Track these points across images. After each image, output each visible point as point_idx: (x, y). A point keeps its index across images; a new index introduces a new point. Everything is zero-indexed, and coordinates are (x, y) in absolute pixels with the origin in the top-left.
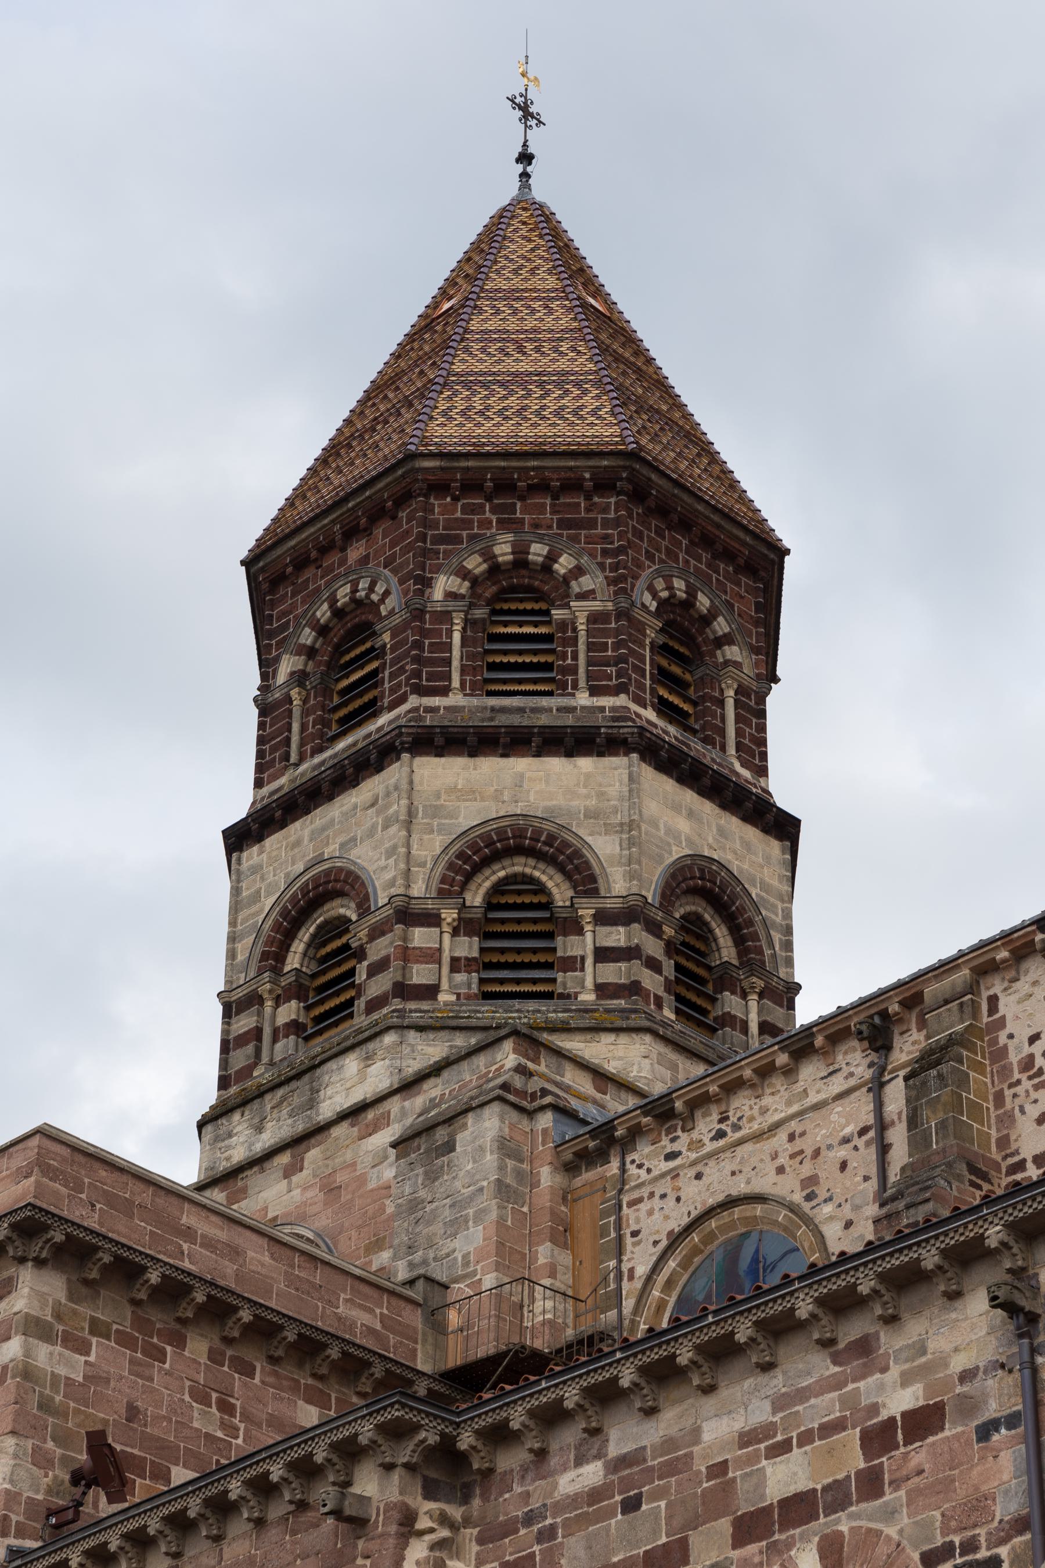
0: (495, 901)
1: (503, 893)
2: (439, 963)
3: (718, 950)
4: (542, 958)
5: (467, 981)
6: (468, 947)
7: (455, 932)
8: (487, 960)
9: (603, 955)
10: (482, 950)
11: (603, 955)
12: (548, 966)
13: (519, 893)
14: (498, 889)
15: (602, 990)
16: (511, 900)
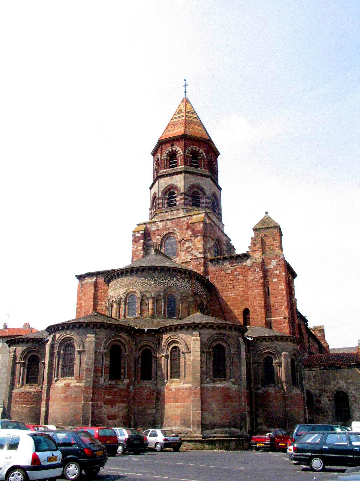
11: (181, 199)
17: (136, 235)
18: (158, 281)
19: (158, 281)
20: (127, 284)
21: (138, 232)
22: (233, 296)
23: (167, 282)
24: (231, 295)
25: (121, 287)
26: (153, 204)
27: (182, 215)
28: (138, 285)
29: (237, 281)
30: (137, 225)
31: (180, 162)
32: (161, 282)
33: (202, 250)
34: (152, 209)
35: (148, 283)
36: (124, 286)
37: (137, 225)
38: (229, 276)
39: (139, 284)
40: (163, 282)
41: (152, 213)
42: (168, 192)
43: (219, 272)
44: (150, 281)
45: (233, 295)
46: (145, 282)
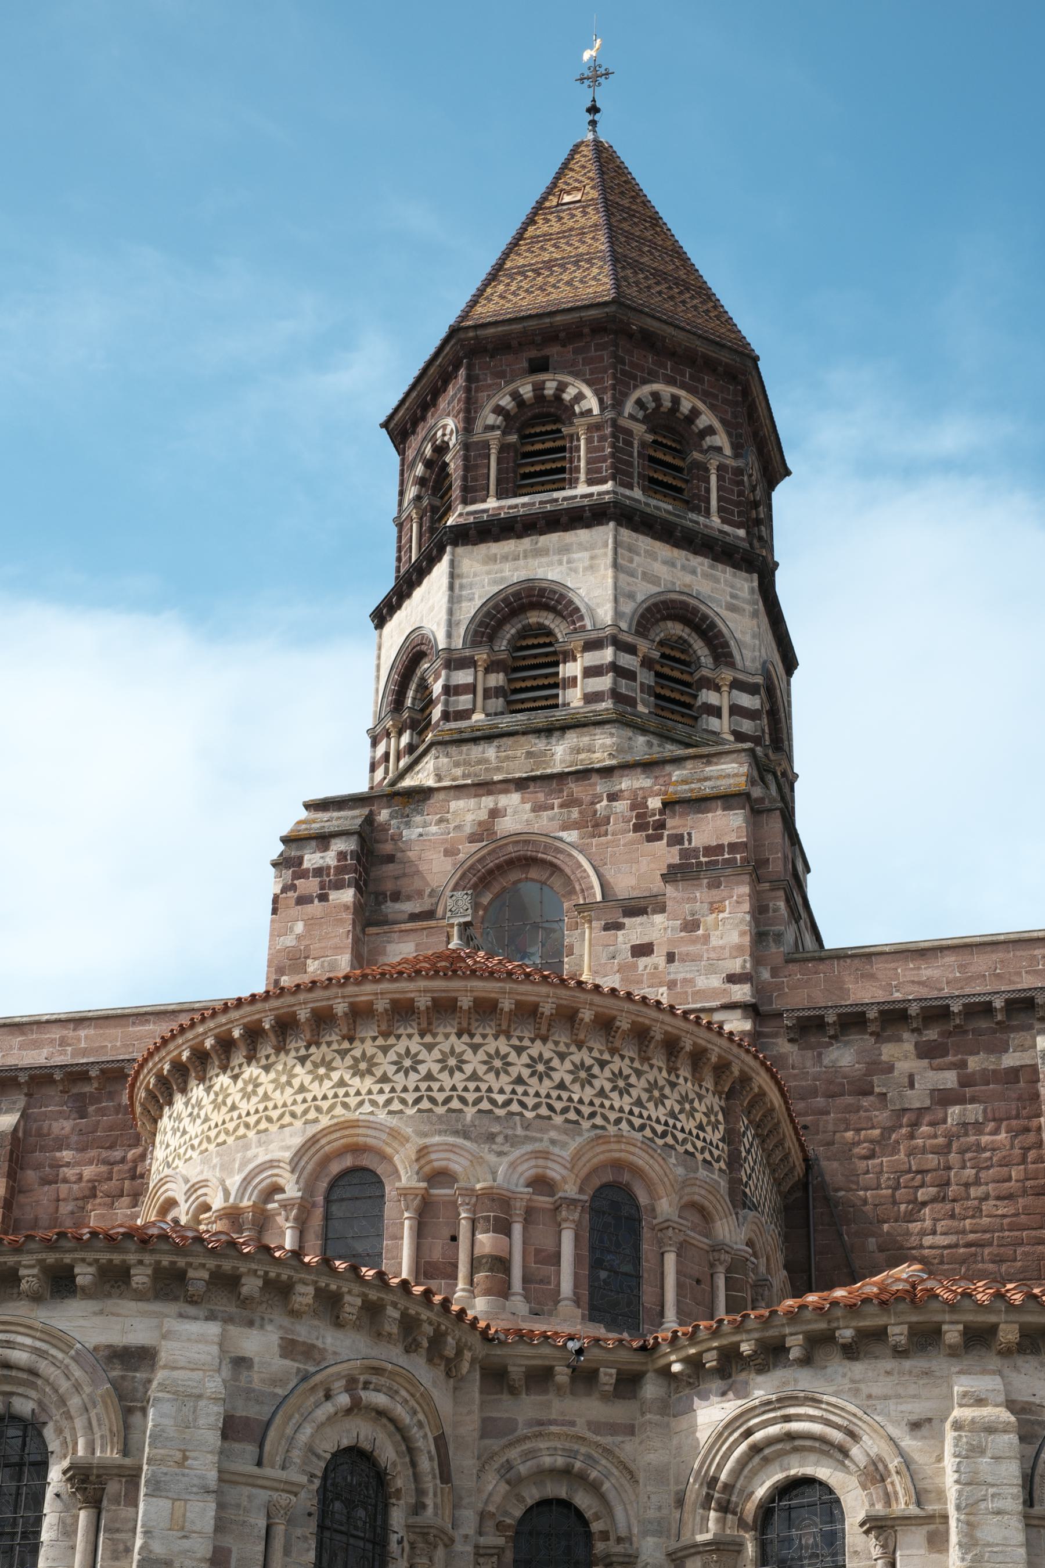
0: (519, 645)
1: (524, 638)
2: (475, 693)
3: (695, 652)
4: (551, 681)
5: (497, 703)
6: (496, 679)
7: (487, 670)
8: (512, 687)
9: (590, 672)
10: (510, 681)
11: (590, 672)
12: (556, 686)
13: (536, 636)
14: (523, 634)
15: (590, 698)
16: (530, 642)
17: (306, 857)
18: (532, 1091)
19: (532, 1091)
20: (315, 1099)
21: (323, 840)
22: (945, 1247)
23: (591, 1103)
24: (928, 1240)
25: (275, 1114)
26: (398, 704)
27: (601, 758)
28: (396, 1106)
29: (968, 1155)
30: (308, 806)
31: (583, 464)
32: (554, 1094)
33: (739, 961)
34: (388, 735)
35: (471, 1097)
36: (299, 1109)
37: (308, 806)
38: (915, 1124)
39: (403, 1101)
40: (565, 1095)
41: (387, 755)
42: (510, 631)
43: (849, 1100)
44: (484, 1087)
45: (941, 1240)
46: (448, 1086)
